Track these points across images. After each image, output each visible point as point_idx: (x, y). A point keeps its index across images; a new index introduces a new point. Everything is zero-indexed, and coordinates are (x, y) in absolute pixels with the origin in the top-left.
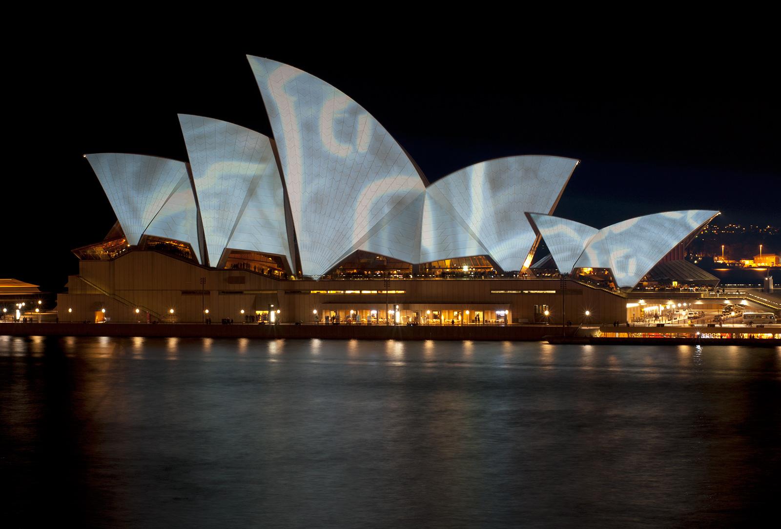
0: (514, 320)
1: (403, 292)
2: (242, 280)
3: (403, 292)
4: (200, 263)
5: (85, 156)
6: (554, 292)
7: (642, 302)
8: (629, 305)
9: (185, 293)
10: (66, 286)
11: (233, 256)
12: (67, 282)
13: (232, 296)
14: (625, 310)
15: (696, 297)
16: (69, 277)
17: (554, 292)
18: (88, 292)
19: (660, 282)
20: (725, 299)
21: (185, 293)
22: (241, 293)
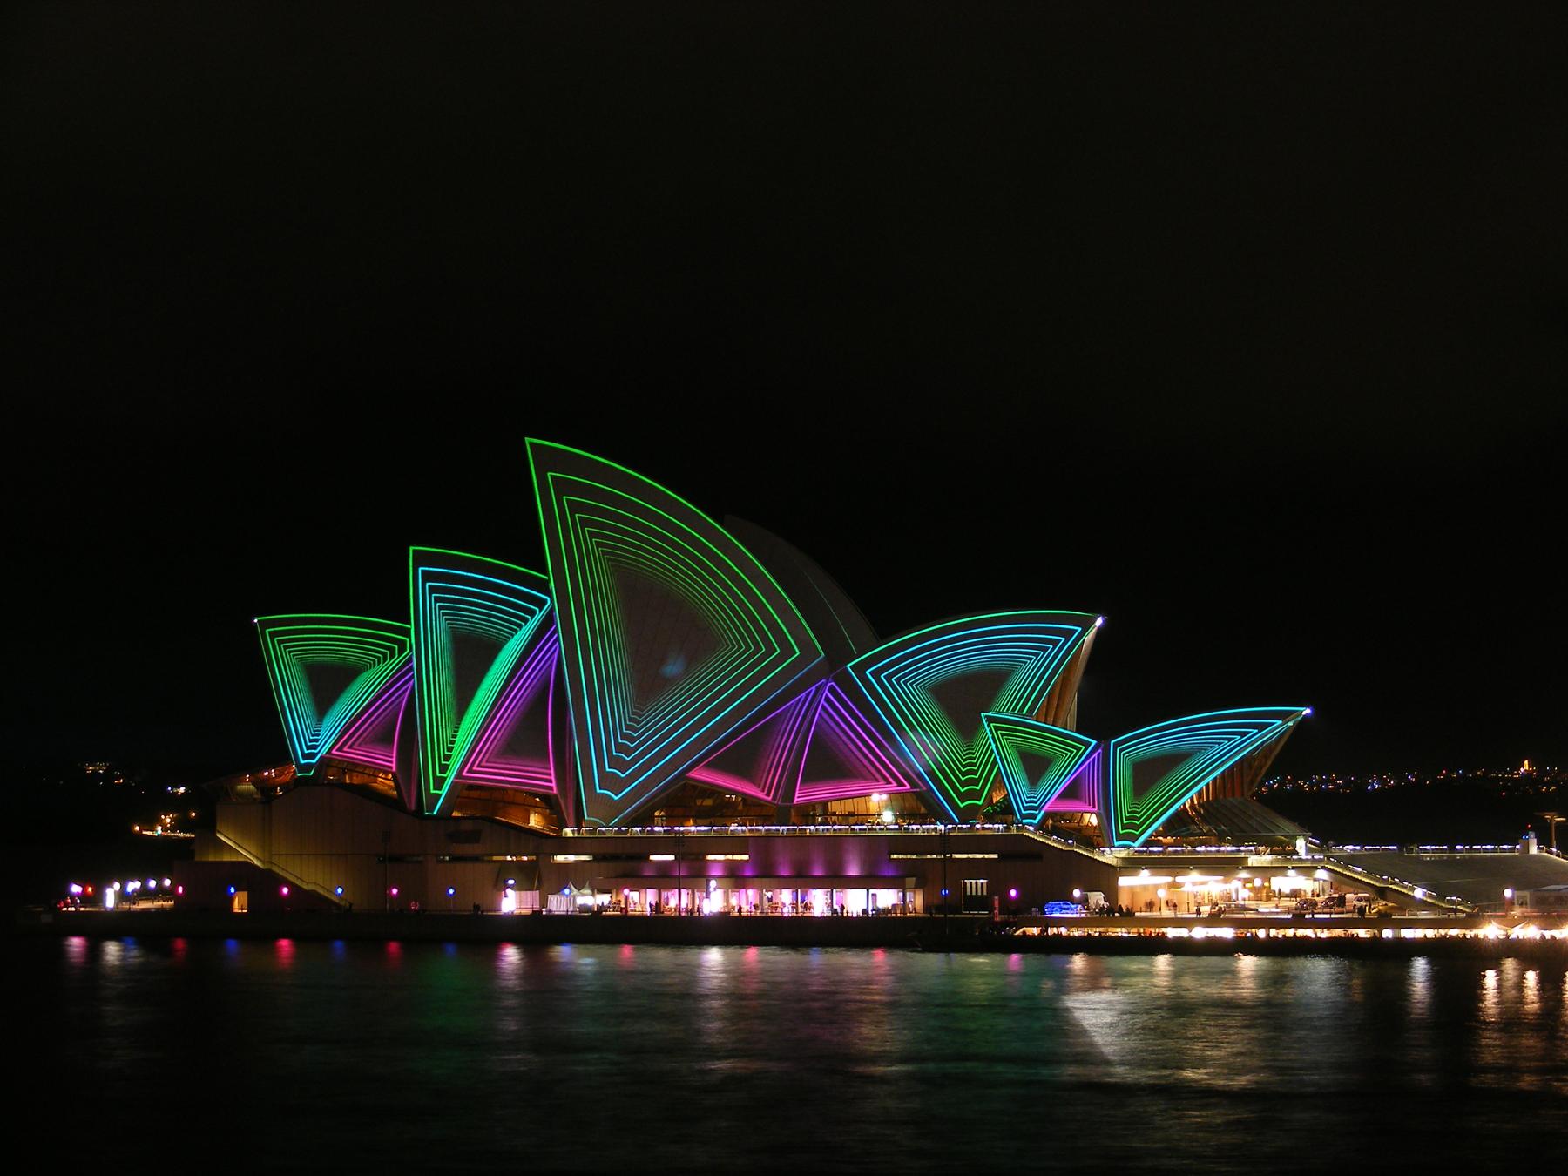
0: (927, 908)
1: (746, 857)
2: (474, 837)
3: (746, 857)
7: (1144, 878)
8: (1124, 881)
13: (459, 866)
18: (227, 858)
22: (476, 859)
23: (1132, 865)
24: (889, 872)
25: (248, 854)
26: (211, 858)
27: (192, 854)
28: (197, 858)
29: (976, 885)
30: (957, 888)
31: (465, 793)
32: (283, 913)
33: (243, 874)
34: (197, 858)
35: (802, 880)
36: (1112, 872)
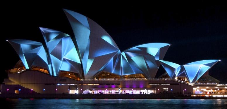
4: (51, 74)
5: (7, 40)
6: (169, 84)
8: (194, 89)
9: (46, 84)
10: (4, 83)
11: (61, 72)
12: (3, 81)
14: (193, 90)
15: (215, 86)
16: (5, 80)
17: (169, 84)
18: (12, 84)
19: (204, 79)
20: (225, 86)
21: (46, 84)
23: (196, 86)
24: (149, 87)
25: (16, 83)
26: (9, 84)
27: (4, 84)
28: (6, 84)
29: (165, 89)
30: (161, 89)
31: (61, 72)
32: (26, 93)
33: (17, 87)
34: (6, 84)
35: (131, 87)
36: (192, 87)
